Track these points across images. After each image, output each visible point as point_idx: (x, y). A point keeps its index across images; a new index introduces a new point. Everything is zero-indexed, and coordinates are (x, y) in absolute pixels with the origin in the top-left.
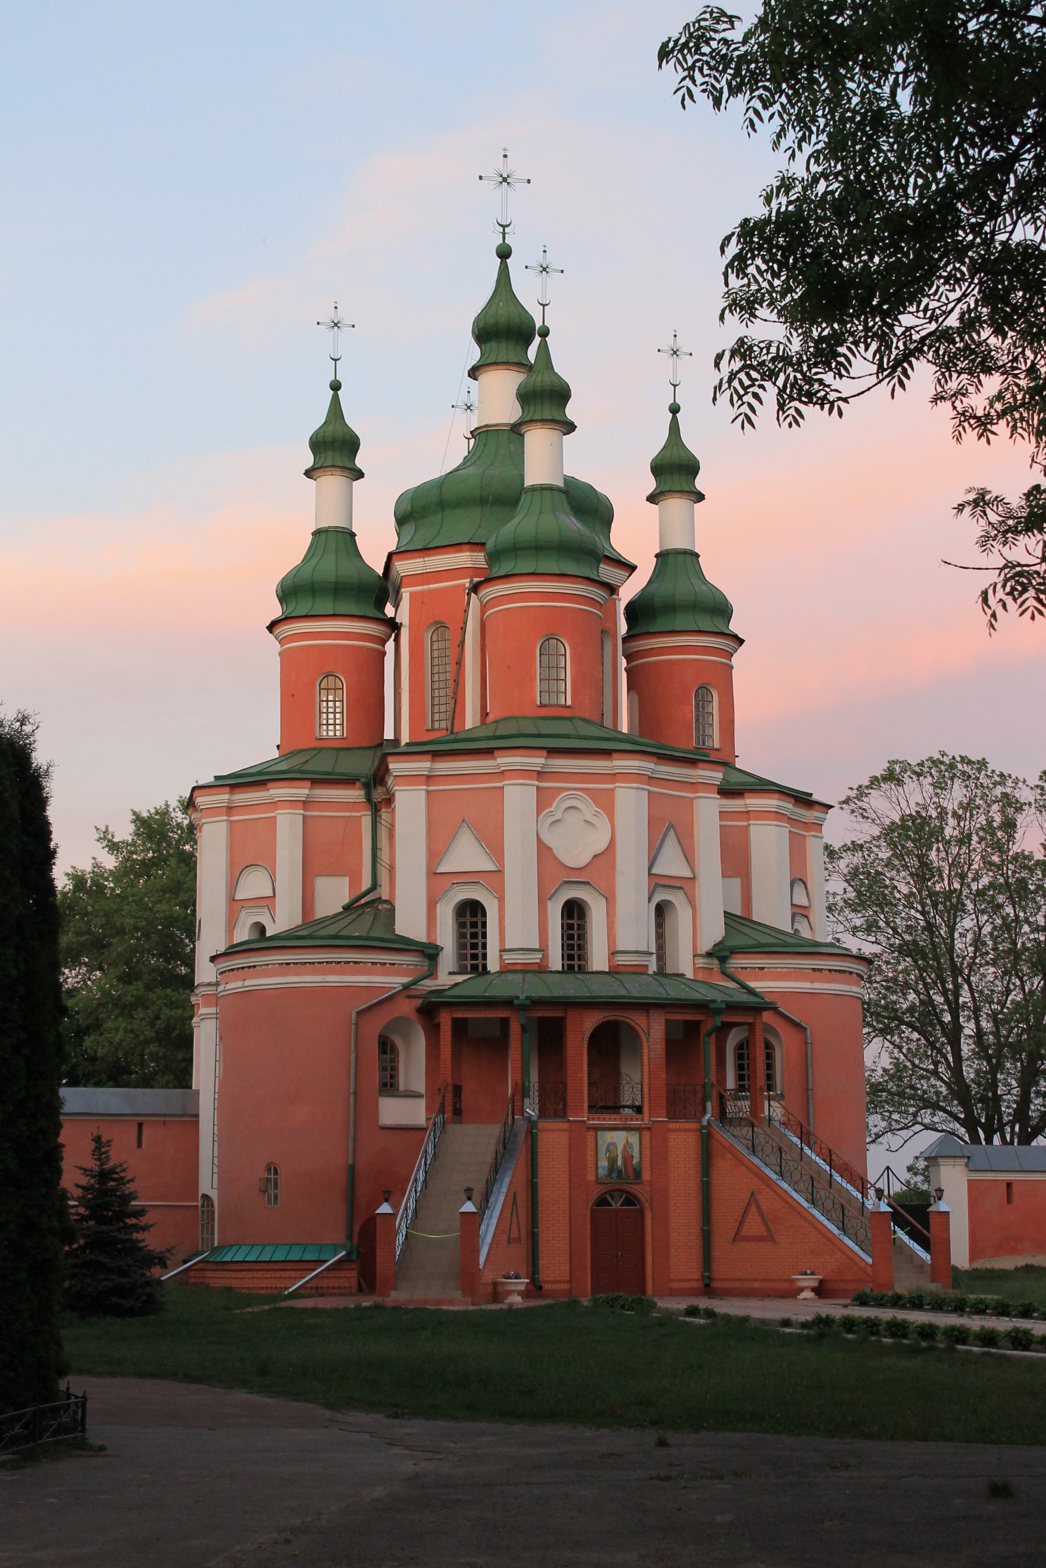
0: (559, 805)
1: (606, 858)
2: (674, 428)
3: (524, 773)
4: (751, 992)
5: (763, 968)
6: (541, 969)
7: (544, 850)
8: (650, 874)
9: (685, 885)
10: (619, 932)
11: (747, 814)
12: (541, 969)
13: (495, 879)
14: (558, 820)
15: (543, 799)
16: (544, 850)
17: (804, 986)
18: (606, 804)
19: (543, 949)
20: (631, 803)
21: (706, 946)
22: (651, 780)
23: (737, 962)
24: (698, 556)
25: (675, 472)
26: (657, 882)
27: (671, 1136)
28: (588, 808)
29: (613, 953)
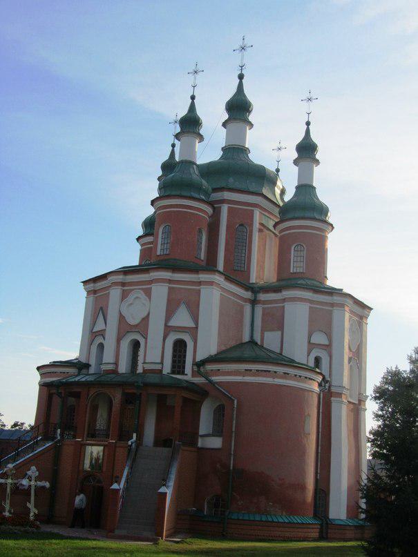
0: (131, 297)
1: (146, 320)
2: (308, 132)
3: (115, 284)
4: (211, 382)
5: (219, 370)
6: (115, 372)
7: (122, 318)
8: (166, 325)
9: (194, 332)
10: (156, 354)
11: (284, 300)
12: (115, 372)
13: (102, 333)
14: (131, 304)
15: (124, 296)
16: (122, 318)
17: (238, 379)
18: (148, 293)
19: (116, 364)
20: (160, 293)
21: (199, 359)
22: (170, 281)
23: (209, 367)
24: (315, 188)
25: (307, 150)
26: (168, 330)
27: (118, 450)
28: (142, 295)
29: (144, 363)
